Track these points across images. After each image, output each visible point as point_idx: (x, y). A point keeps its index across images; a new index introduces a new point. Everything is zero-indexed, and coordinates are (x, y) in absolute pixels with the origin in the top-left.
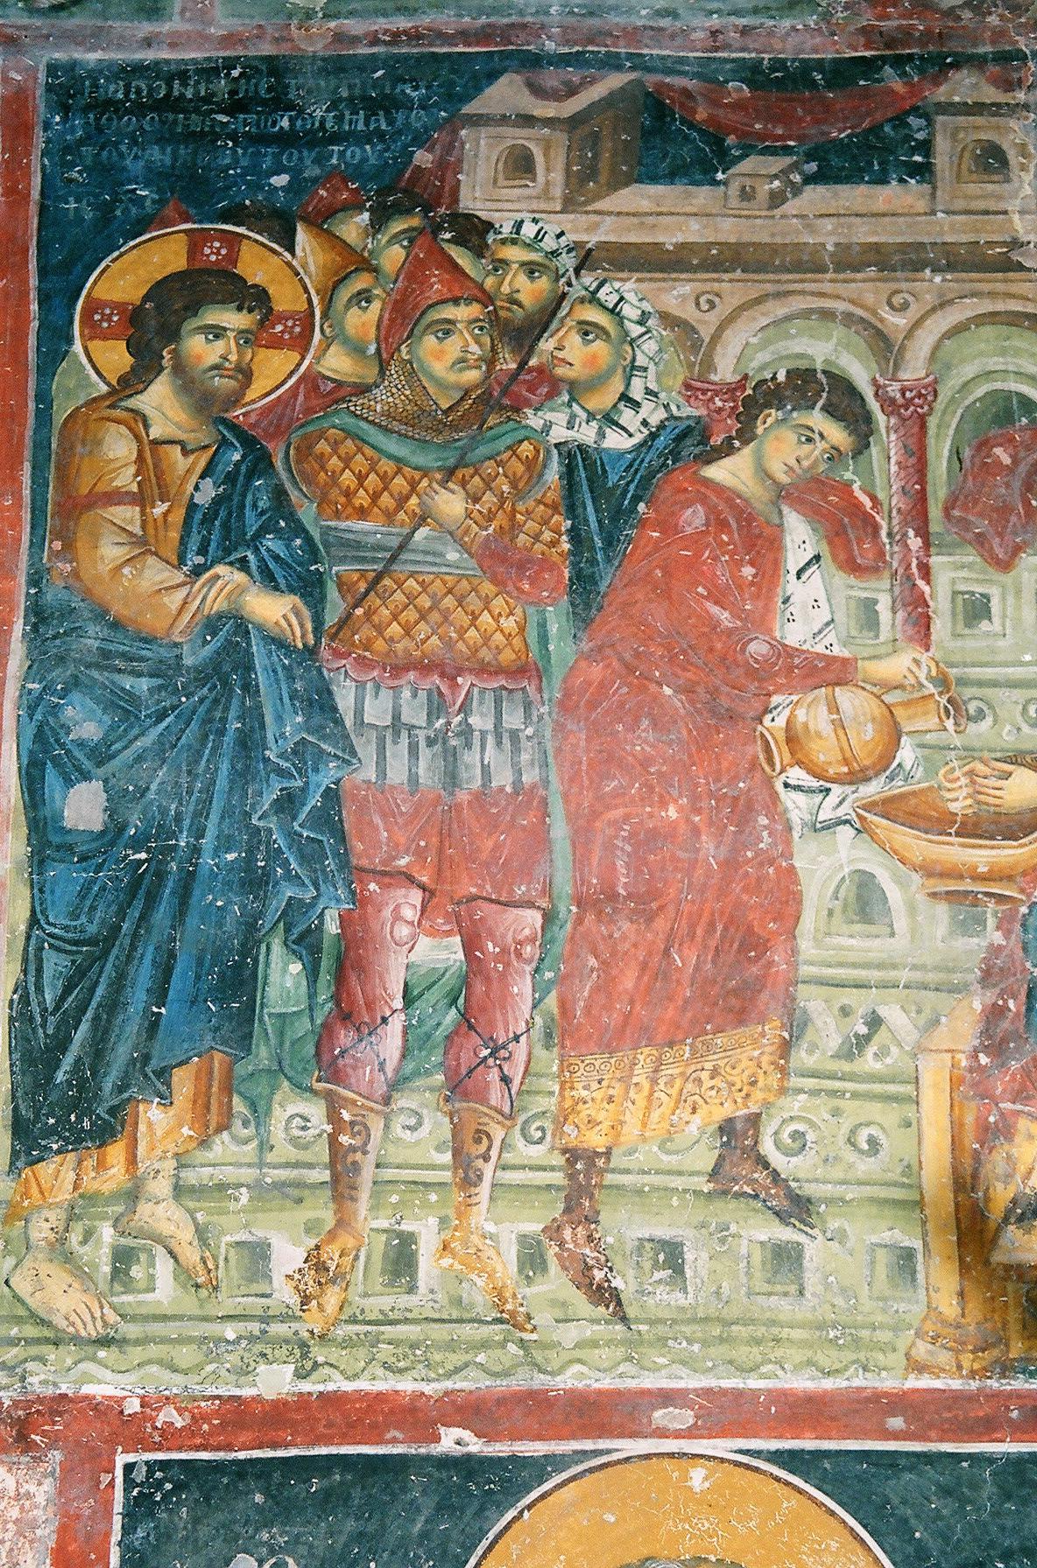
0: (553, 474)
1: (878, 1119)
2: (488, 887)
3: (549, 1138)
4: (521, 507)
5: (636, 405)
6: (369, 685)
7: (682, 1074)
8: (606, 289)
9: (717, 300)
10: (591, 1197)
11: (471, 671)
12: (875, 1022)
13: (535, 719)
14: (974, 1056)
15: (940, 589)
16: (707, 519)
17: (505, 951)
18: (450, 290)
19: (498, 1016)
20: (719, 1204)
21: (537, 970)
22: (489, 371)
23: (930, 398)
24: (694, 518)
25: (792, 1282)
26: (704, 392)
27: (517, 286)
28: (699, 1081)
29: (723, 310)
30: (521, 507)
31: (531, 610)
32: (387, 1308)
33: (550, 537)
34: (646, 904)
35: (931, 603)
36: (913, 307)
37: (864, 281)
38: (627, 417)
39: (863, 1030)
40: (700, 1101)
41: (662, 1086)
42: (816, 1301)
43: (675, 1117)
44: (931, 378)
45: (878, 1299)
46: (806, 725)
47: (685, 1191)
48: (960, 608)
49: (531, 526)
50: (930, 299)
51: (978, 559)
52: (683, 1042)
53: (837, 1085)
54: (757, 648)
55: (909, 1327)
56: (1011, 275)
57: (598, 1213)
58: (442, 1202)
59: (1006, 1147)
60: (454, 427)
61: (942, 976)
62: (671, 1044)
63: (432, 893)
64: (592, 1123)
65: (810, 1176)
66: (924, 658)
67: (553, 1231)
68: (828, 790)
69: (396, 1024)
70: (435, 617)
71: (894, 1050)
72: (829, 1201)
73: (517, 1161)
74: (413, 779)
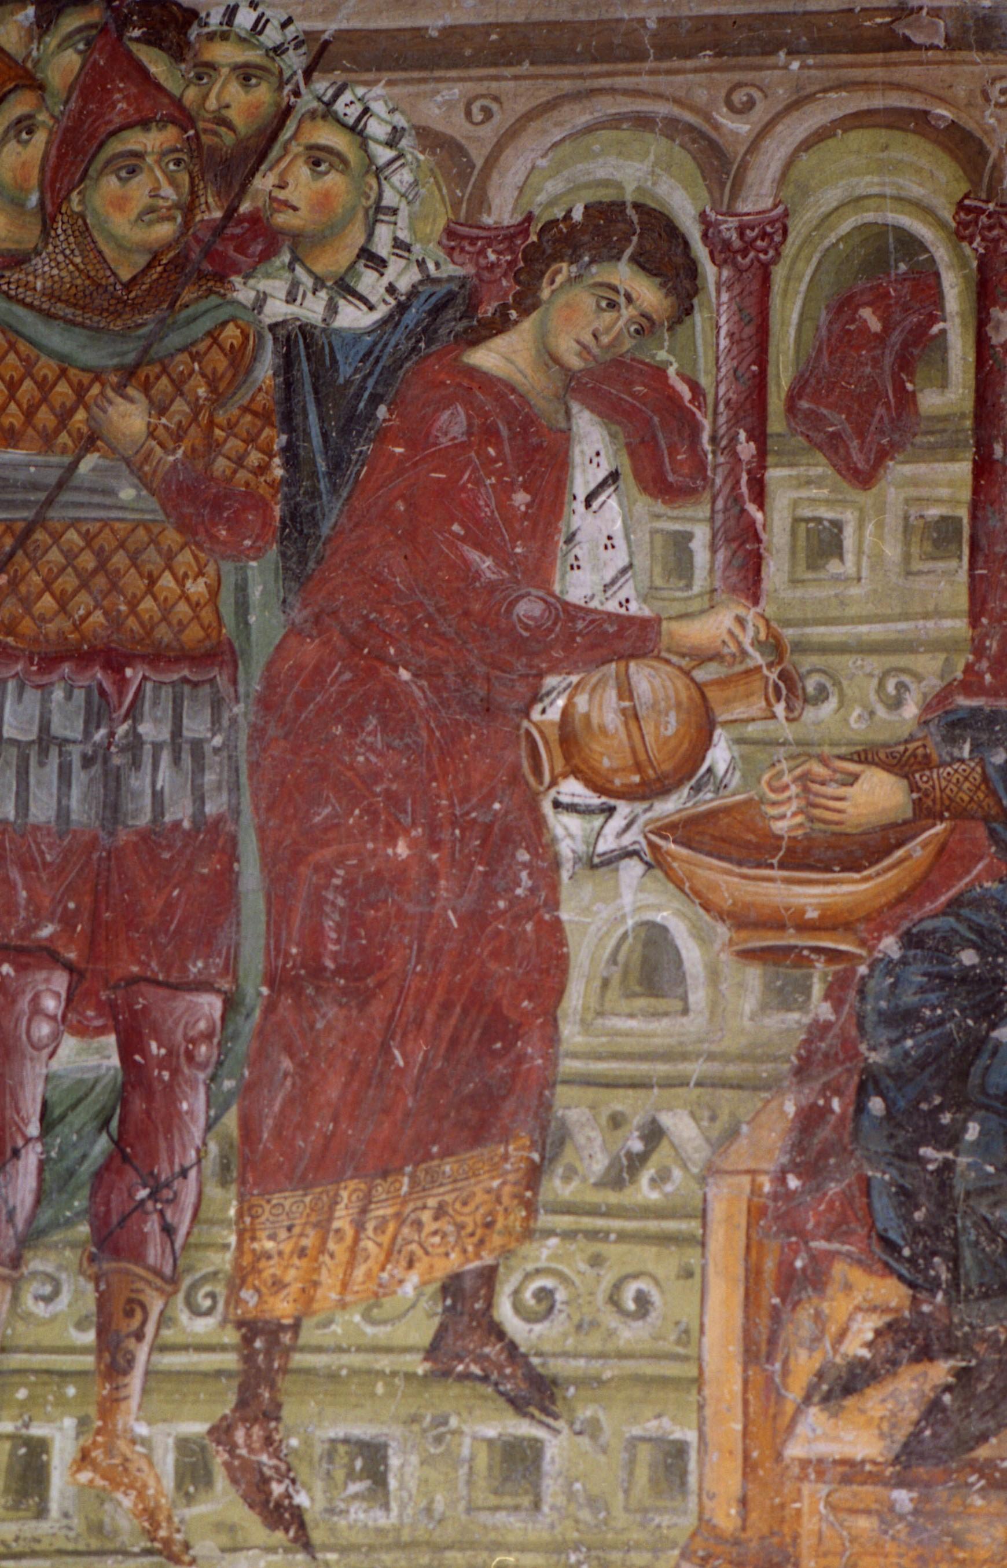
0: (265, 370)
1: (650, 1267)
2: (154, 964)
3: (221, 1306)
4: (221, 417)
5: (379, 264)
6: (11, 685)
7: (397, 1215)
8: (347, 96)
9: (495, 107)
10: (272, 1386)
11: (143, 658)
12: (654, 1134)
13: (225, 723)
14: (781, 1179)
15: (776, 516)
16: (470, 425)
17: (170, 1053)
18: (138, 110)
19: (163, 1145)
20: (437, 1390)
21: (213, 1078)
22: (187, 224)
23: (777, 238)
24: (453, 424)
25: (526, 1492)
26: (473, 240)
27: (227, 99)
28: (418, 1225)
29: (501, 120)
30: (221, 417)
31: (227, 567)
32: (9, 1537)
33: (255, 461)
34: (361, 975)
35: (764, 537)
36: (760, 107)
37: (695, 71)
38: (368, 282)
39: (637, 1146)
40: (419, 1252)
41: (370, 1232)
42: (555, 1516)
43: (385, 1275)
44: (780, 209)
45: (636, 1511)
46: (587, 717)
47: (394, 1374)
48: (802, 542)
49: (233, 445)
50: (782, 94)
51: (830, 471)
52: (400, 1171)
53: (600, 1223)
54: (529, 608)
55: (674, 1545)
56: (894, 56)
57: (279, 1406)
58: (83, 1396)
59: (815, 1301)
60: (137, 307)
61: (747, 1067)
62: (385, 1175)
63: (81, 974)
64: (278, 1285)
65: (558, 1349)
66: (751, 615)
67: (222, 1432)
68: (611, 810)
69: (30, 1159)
70: (100, 582)
71: (677, 1173)
72: (584, 1382)
73: (180, 1339)
74: (63, 813)
